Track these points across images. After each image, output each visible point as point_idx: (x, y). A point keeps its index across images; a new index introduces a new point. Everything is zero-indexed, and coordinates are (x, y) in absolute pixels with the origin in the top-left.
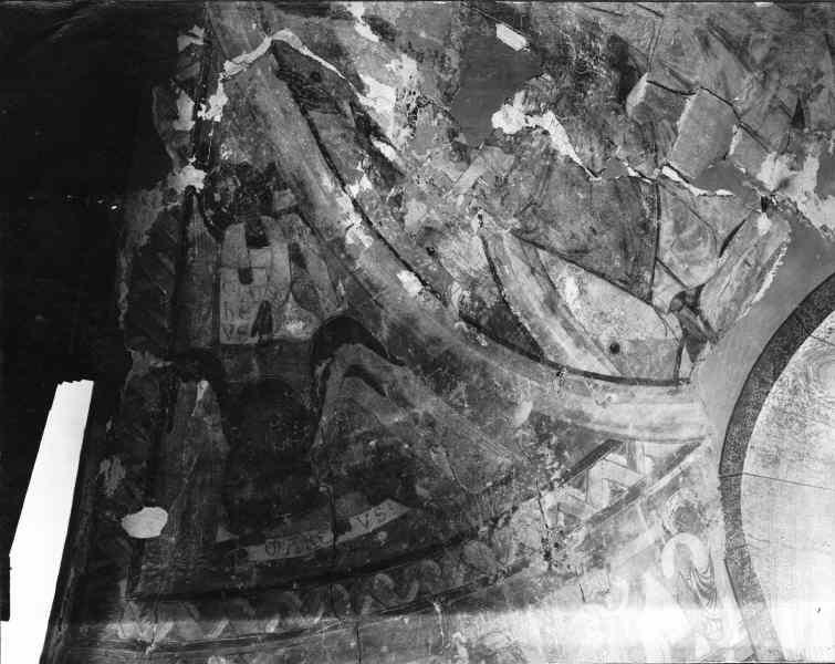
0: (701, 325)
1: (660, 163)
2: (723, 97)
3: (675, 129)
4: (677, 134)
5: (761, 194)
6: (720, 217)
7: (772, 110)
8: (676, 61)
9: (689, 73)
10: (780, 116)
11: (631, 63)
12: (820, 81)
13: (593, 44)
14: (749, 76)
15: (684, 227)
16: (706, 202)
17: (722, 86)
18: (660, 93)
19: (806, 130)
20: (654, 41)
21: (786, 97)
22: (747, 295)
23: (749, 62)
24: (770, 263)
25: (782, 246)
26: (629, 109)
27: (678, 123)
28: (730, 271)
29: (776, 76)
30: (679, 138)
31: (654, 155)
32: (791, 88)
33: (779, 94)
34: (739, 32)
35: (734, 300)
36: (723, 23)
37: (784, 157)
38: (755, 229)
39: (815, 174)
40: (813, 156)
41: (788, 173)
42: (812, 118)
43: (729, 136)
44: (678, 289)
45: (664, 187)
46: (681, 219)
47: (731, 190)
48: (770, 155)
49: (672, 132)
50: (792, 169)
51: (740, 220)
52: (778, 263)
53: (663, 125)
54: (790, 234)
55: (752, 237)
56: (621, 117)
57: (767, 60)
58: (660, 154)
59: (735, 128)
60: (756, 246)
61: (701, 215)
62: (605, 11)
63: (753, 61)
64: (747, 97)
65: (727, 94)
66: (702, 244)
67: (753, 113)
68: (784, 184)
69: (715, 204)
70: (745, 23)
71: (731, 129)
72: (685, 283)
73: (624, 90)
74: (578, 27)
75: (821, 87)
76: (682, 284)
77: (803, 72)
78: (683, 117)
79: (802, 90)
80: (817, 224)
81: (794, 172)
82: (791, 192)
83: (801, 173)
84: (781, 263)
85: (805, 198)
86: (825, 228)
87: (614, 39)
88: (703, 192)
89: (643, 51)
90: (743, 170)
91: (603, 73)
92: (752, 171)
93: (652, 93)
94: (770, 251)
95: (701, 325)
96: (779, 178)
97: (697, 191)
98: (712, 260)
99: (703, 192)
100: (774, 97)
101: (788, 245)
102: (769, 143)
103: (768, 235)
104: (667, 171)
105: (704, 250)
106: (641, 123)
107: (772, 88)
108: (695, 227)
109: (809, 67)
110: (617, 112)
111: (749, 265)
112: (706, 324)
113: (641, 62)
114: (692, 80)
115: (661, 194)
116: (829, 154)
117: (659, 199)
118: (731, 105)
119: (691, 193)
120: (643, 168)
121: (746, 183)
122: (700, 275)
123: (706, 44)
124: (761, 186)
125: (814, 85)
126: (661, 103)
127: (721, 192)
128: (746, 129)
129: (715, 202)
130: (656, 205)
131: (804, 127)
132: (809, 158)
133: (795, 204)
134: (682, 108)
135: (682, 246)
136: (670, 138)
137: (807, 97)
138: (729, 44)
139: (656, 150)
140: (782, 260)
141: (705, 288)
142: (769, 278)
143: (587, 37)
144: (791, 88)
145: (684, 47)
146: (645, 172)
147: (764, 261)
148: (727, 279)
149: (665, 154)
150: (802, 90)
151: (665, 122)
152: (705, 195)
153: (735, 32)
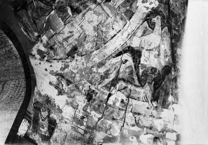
0: (18, 8)
1: (55, 10)
2: (61, 32)
3: (59, 17)
4: (59, 17)
5: (42, 35)
6: (40, 22)
7: (55, 42)
8: (71, 24)
9: (67, 26)
10: (53, 44)
11: (75, 13)
12: (56, 55)
13: (83, 6)
14: (62, 39)
15: (41, 11)
16: (44, 19)
17: (63, 33)
18: (67, 17)
19: (49, 49)
20: (76, 21)
21: (56, 46)
22: (23, 26)
23: (64, 40)
24: (29, 35)
25: (31, 39)
26: (68, 7)
27: (60, 18)
28: (29, 21)
29: (60, 46)
30: (58, 18)
31: (57, 9)
32: (56, 48)
33: (57, 45)
34: (69, 40)
35: (23, 21)
36: (72, 38)
37: (46, 43)
38: (35, 31)
39: (41, 49)
40: (45, 50)
41: (43, 43)
42: (51, 51)
43: (54, 30)
44: (28, 3)
45: (50, 8)
46: (43, 11)
47: (45, 27)
48: (47, 39)
49: (59, 16)
50: (44, 44)
51: (38, 28)
52: (28, 36)
53: (61, 14)
54: (33, 41)
55: (34, 30)
56: (68, 4)
57: (63, 44)
58: (57, 11)
59: (54, 32)
60: (32, 30)
61: (42, 17)
62: (86, 12)
63: (64, 41)
64: (58, 38)
65: (61, 33)
66: (36, 15)
67: (56, 38)
68: (42, 41)
69: (43, 21)
70: (70, 43)
71: (55, 32)
72: (29, 6)
73: (72, 8)
74: (87, 4)
75: (55, 55)
76: (29, 5)
77: (58, 52)
78: (61, 20)
79: (56, 50)
80: (33, 49)
81: (43, 44)
82: (40, 42)
83: (42, 46)
84: (28, 37)
85: (38, 46)
86: (32, 50)
87: (81, 11)
88: (46, 19)
89: (76, 17)
90: (47, 32)
91: (77, 4)
92: (46, 34)
93: (68, 15)
94: (30, 35)
95: (18, 8)
96: (43, 40)
97: (47, 18)
98: (32, 16)
99: (46, 19)
100: (57, 44)
101: (31, 40)
102: (49, 40)
103: (34, 35)
104: (53, 11)
105: (35, 15)
106: (65, 9)
107: (58, 44)
108: (40, 14)
109: (59, 53)
110: (69, 4)
111: (29, 27)
112: (19, 10)
113: (75, 15)
114: (66, 26)
115: (49, 7)
116: (44, 54)
117: (49, 6)
118: (59, 33)
119: (47, 16)
120: (56, 5)
121: (45, 32)
122: (29, 12)
123: (70, 32)
124: (43, 35)
125: (56, 53)
126: (66, 16)
127: (45, 24)
128: (53, 35)
129: (43, 22)
130: (47, 4)
131: (50, 49)
132: (44, 49)
133: (38, 43)
134: (63, 21)
135: (37, 8)
136: (59, 15)
137: (54, 51)
138: (68, 37)
139: (58, 10)
140: (29, 38)
141: (26, 11)
142: (26, 34)
143: (84, 5)
144: (56, 48)
145: (72, 27)
146: (55, 5)
147: (29, 32)
148: (27, 20)
149: (56, 12)
150: (56, 50)
151: (61, 15)
152: (45, 20)
153: (70, 39)
